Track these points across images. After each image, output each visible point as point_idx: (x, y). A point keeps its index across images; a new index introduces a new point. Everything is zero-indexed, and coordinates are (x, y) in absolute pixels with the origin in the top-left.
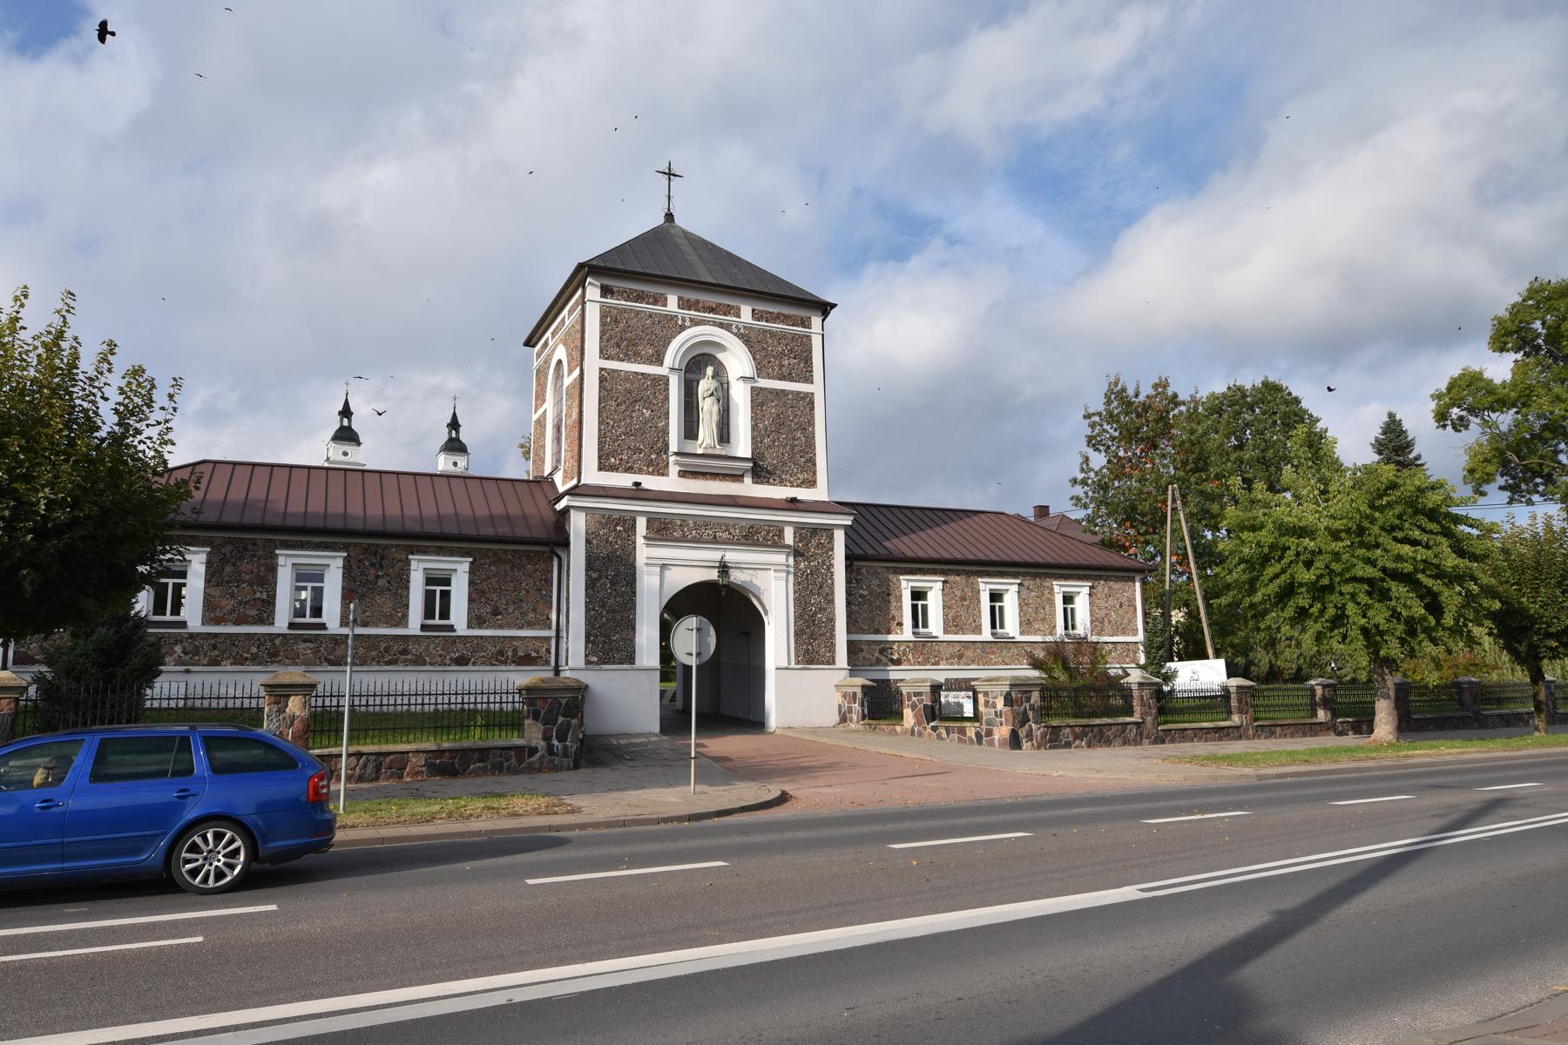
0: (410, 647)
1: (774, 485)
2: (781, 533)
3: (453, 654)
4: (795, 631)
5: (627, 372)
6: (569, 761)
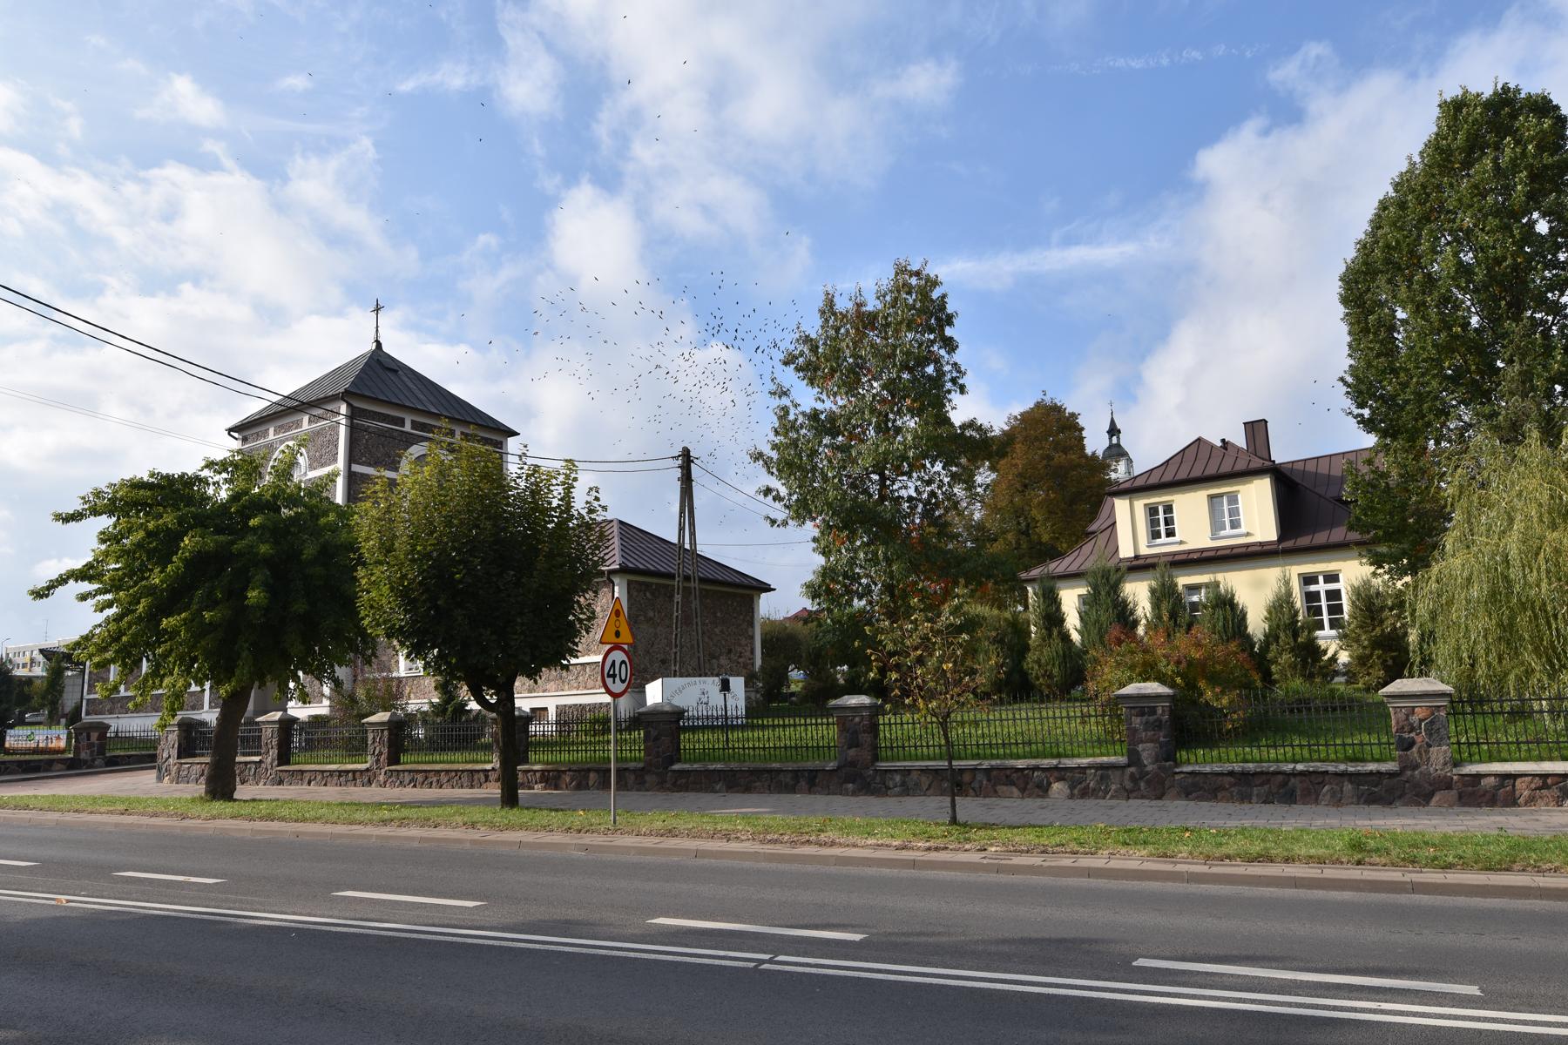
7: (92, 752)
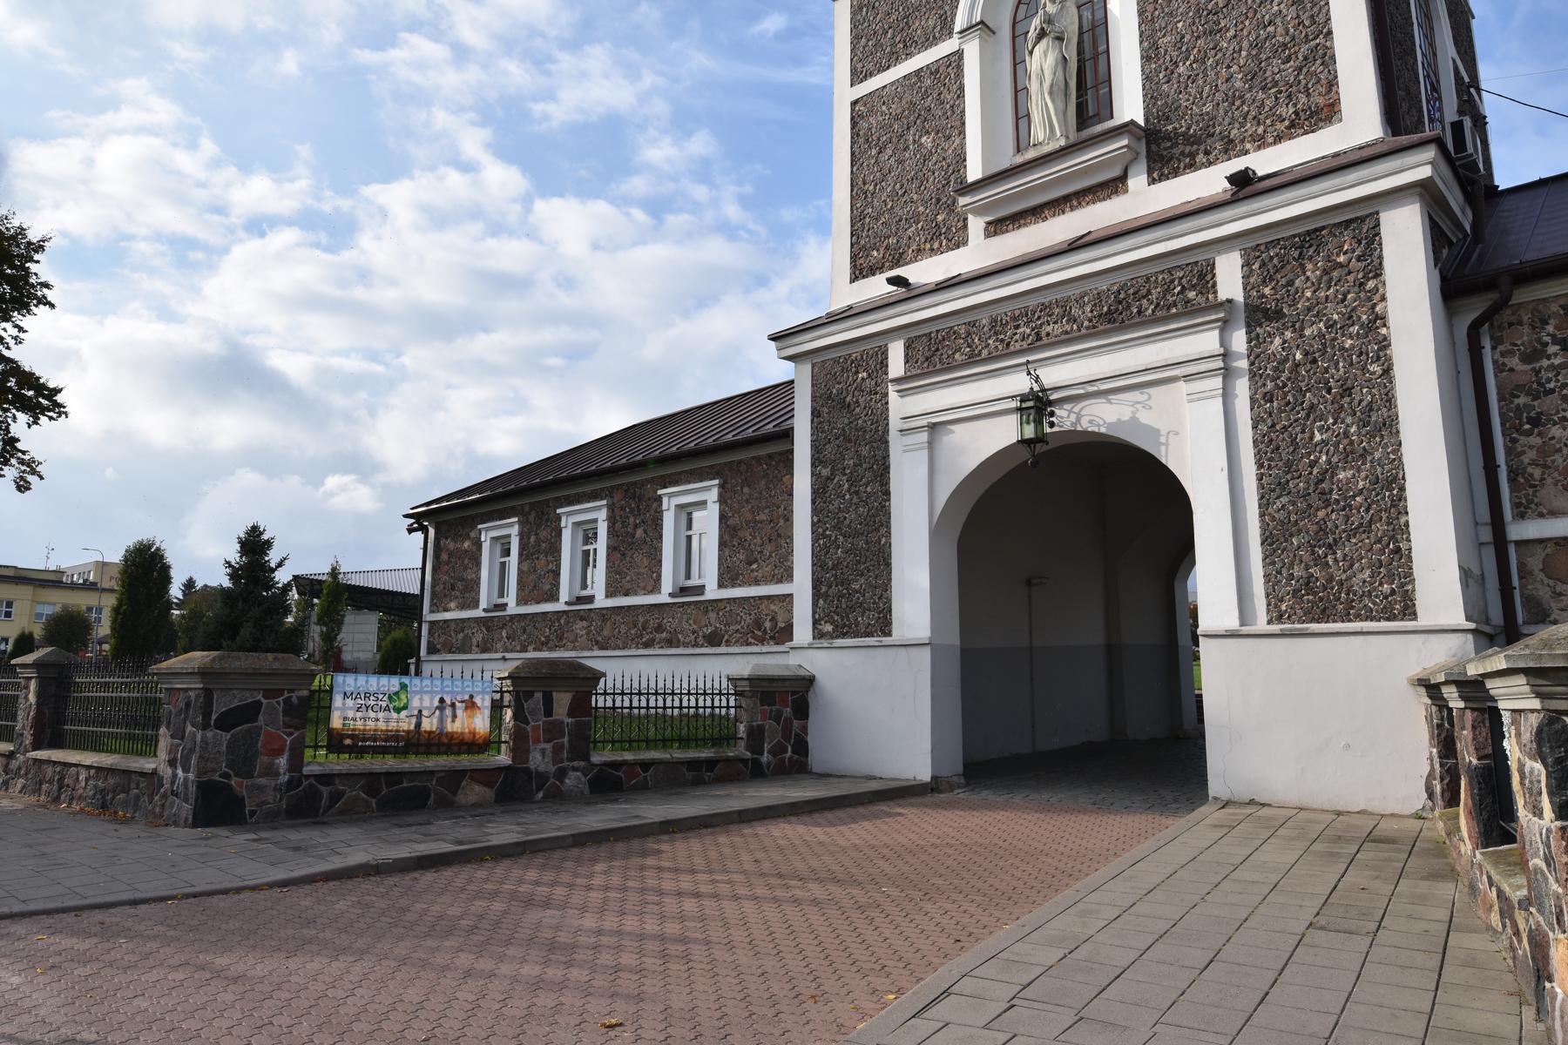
0: (665, 621)
1: (1210, 164)
2: (1205, 277)
3: (705, 629)
4: (1264, 528)
5: (892, 84)
6: (186, 809)
7: (558, 749)
